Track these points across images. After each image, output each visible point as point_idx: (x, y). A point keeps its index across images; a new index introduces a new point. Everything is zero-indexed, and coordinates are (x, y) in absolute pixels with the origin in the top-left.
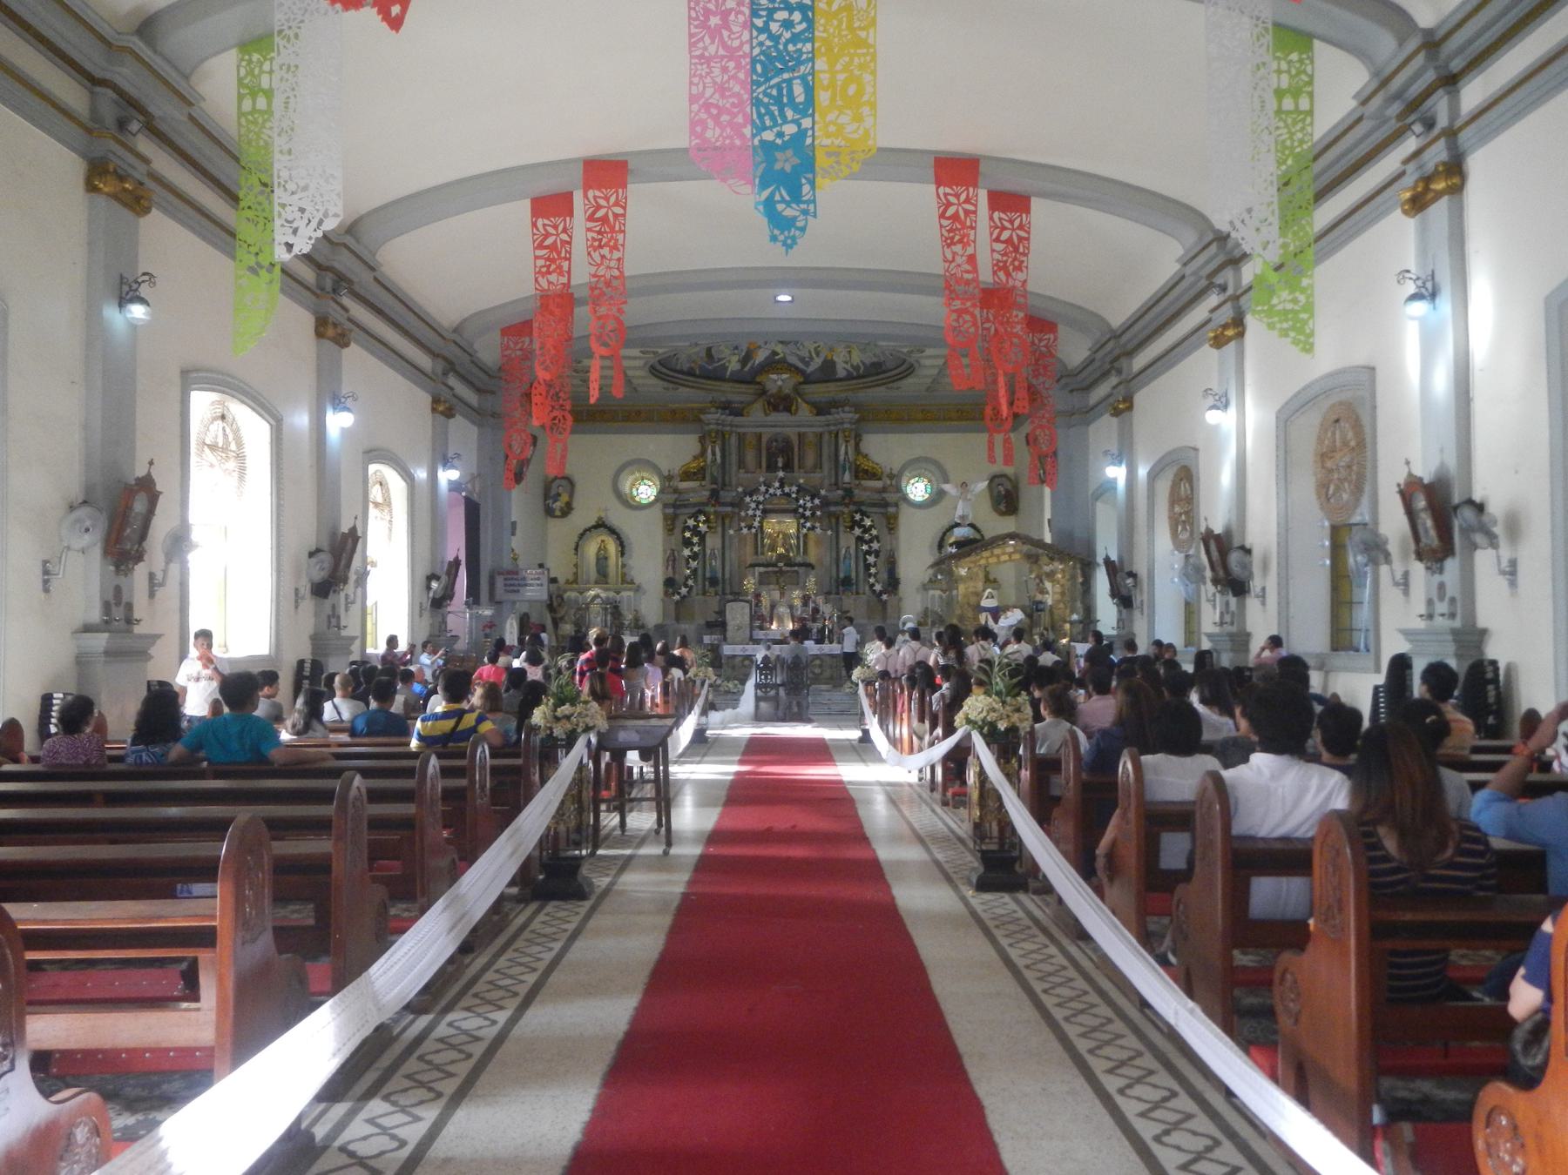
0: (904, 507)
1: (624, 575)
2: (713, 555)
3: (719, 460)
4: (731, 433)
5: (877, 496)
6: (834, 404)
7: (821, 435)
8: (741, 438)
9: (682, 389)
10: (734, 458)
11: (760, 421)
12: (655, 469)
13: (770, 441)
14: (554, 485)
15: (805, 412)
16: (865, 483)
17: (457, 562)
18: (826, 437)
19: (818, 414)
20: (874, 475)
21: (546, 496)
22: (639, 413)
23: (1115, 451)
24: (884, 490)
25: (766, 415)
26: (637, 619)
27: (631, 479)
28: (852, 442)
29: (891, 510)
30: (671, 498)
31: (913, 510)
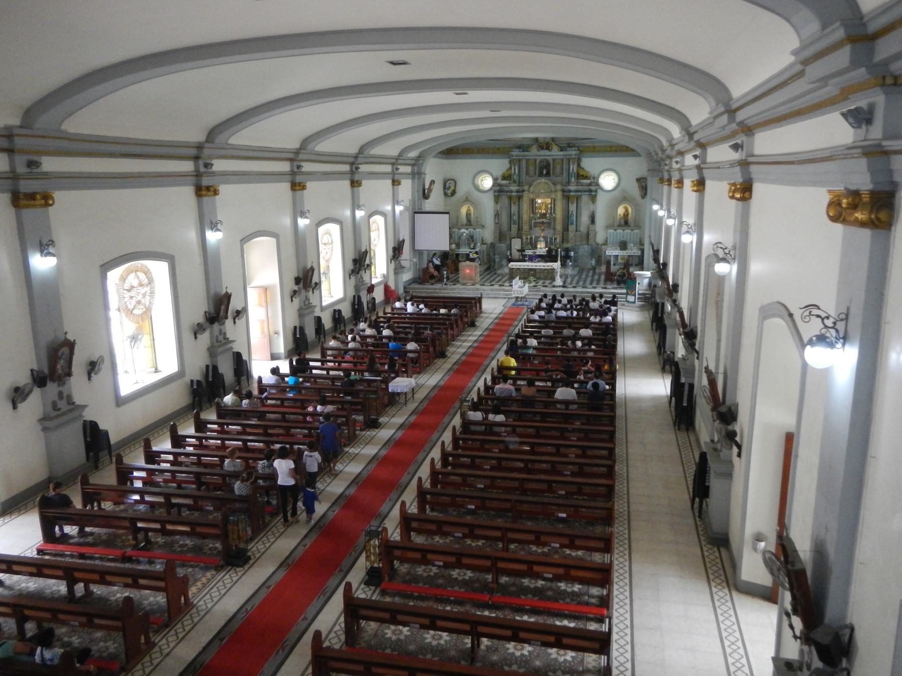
0: (599, 191)
1: (477, 222)
2: (514, 214)
3: (517, 172)
4: (522, 159)
5: (586, 188)
7: (562, 160)
8: (527, 161)
10: (524, 170)
13: (540, 162)
14: (448, 184)
16: (581, 181)
18: (565, 161)
19: (561, 151)
21: (445, 188)
22: (483, 149)
24: (590, 185)
25: (538, 151)
26: (483, 240)
27: (481, 178)
28: (576, 164)
29: (593, 193)
31: (604, 193)
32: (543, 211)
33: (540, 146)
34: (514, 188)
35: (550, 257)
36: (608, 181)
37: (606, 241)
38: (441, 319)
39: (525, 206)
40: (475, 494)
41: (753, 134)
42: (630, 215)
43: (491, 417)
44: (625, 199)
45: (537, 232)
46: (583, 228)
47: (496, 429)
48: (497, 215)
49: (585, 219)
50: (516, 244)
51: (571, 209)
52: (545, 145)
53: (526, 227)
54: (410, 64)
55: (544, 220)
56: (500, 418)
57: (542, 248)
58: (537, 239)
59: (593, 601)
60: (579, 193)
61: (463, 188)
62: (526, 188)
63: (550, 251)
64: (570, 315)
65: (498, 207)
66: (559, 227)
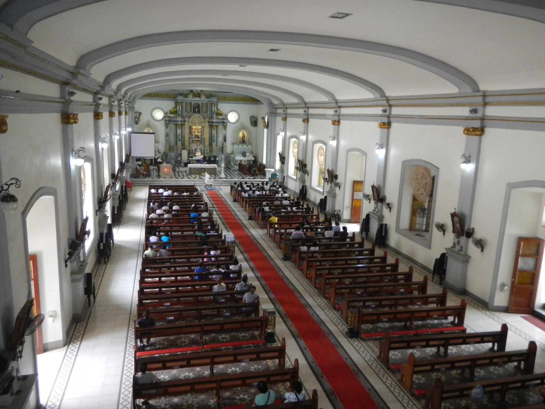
0: (228, 123)
2: (179, 135)
8: (186, 103)
13: (194, 104)
15: (203, 98)
18: (209, 104)
20: (221, 115)
22: (157, 94)
23: (282, 129)
24: (223, 119)
29: (225, 124)
30: (167, 119)
31: (231, 124)
33: (194, 95)
35: (206, 160)
36: (232, 117)
37: (233, 152)
38: (186, 199)
39: (187, 131)
40: (346, 286)
41: (486, 106)
42: (246, 138)
43: (312, 249)
44: (243, 128)
45: (194, 146)
46: (220, 144)
47: (315, 255)
48: (167, 135)
49: (220, 139)
50: (185, 154)
51: (213, 133)
52: (198, 95)
53: (187, 143)
54: (280, 49)
55: (199, 139)
56: (317, 248)
57: (199, 156)
58: (196, 150)
59: (449, 325)
60: (218, 124)
61: (144, 119)
63: (205, 157)
64: (262, 194)
66: (207, 143)
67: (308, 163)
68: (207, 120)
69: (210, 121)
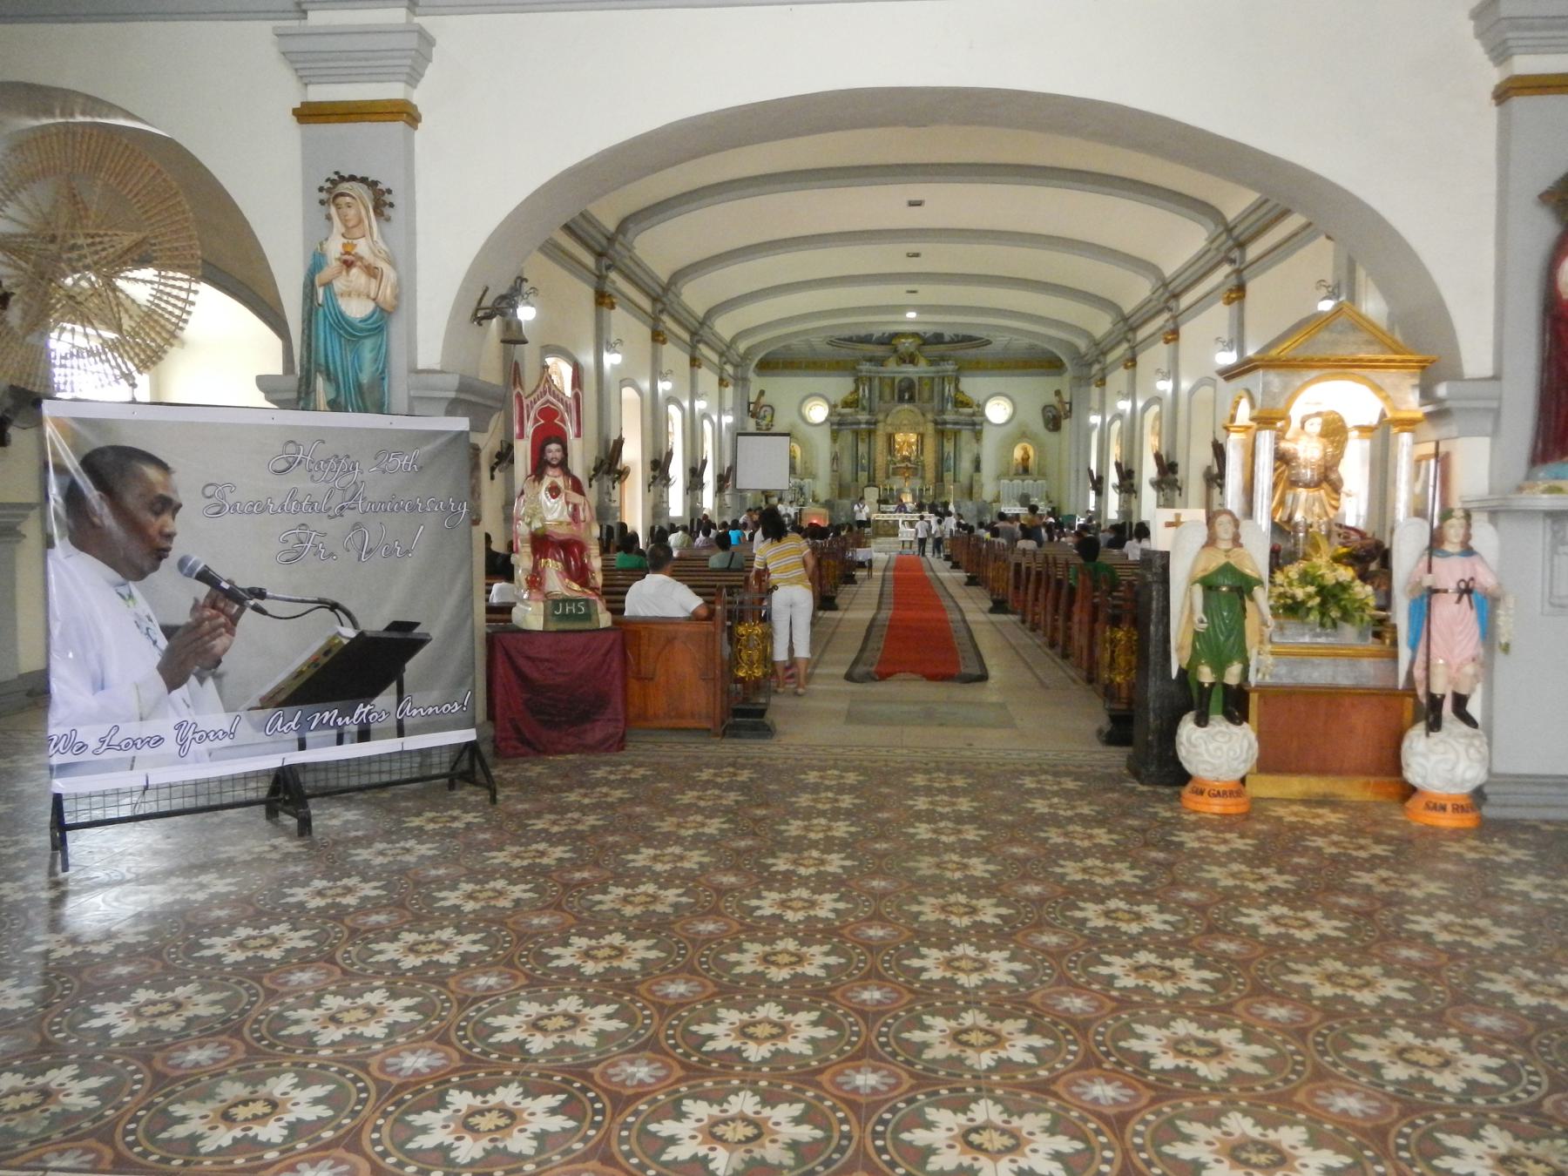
6: (943, 359)
7: (932, 379)
9: (843, 351)
10: (877, 393)
11: (893, 368)
12: (827, 400)
17: (730, 469)
20: (967, 405)
24: (973, 414)
30: (836, 419)
32: (905, 453)
34: (863, 417)
36: (997, 411)
44: (1024, 435)
45: (897, 483)
46: (964, 478)
48: (835, 459)
49: (966, 465)
53: (880, 475)
62: (881, 417)
65: (837, 448)
66: (930, 474)
67: (1136, 468)
68: (930, 416)
69: (939, 419)
